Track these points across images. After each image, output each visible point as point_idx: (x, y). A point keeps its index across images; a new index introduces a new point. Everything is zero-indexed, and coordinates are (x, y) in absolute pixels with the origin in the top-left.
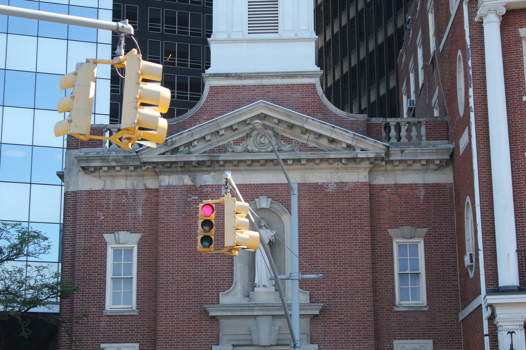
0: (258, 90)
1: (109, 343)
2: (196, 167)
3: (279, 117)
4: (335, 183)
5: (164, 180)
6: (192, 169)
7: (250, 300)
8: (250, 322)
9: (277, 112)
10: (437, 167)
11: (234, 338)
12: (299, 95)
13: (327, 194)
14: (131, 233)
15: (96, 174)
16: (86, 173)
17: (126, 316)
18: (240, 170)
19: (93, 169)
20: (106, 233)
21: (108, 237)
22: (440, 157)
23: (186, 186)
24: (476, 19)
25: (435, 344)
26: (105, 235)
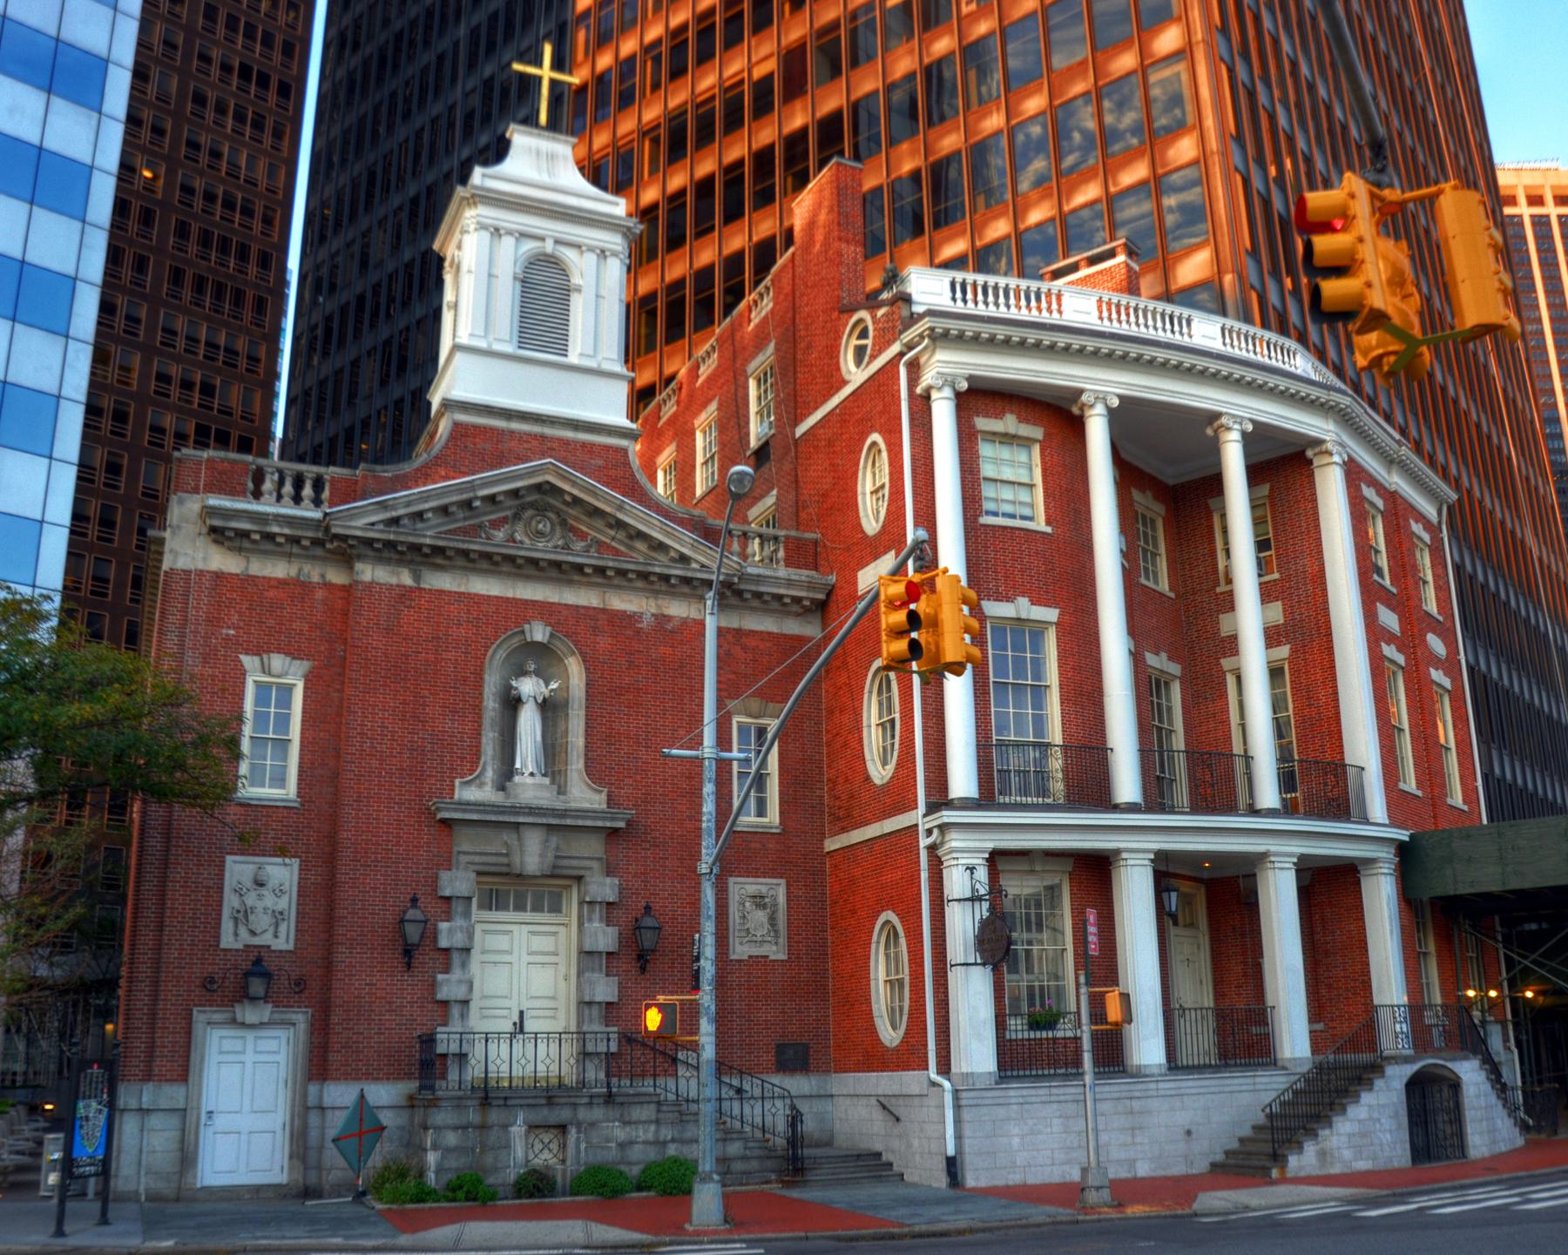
0: (535, 443)
1: (242, 854)
2: (426, 555)
3: (575, 492)
4: (653, 615)
5: (363, 572)
6: (418, 559)
7: (508, 796)
8: (508, 837)
9: (574, 484)
10: (801, 610)
11: (477, 859)
12: (600, 462)
13: (639, 631)
14: (294, 658)
15: (237, 543)
16: (216, 541)
17: (277, 807)
18: (500, 573)
19: (232, 534)
20: (247, 654)
21: (249, 661)
22: (811, 595)
23: (404, 587)
24: (919, 390)
25: (788, 886)
26: (242, 657)
